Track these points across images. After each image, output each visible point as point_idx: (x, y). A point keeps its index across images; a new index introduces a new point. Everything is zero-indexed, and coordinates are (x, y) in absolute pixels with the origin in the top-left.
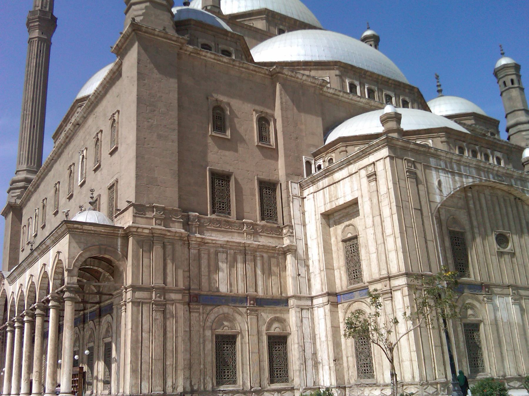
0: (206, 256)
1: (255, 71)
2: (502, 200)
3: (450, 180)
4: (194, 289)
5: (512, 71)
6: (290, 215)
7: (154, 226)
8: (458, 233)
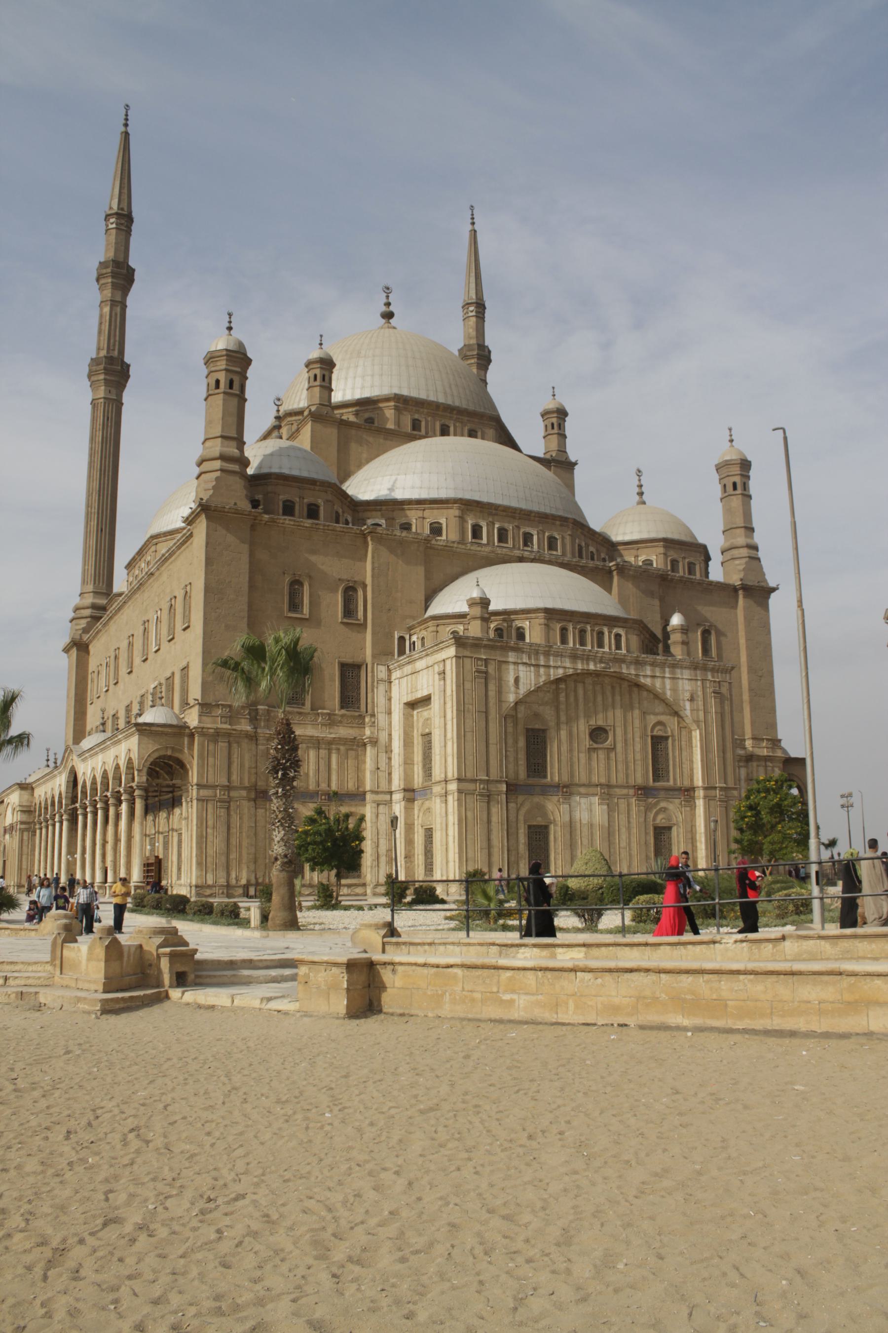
2: (609, 688)
3: (533, 674)
5: (736, 470)
6: (373, 702)
7: (220, 726)
8: (539, 730)
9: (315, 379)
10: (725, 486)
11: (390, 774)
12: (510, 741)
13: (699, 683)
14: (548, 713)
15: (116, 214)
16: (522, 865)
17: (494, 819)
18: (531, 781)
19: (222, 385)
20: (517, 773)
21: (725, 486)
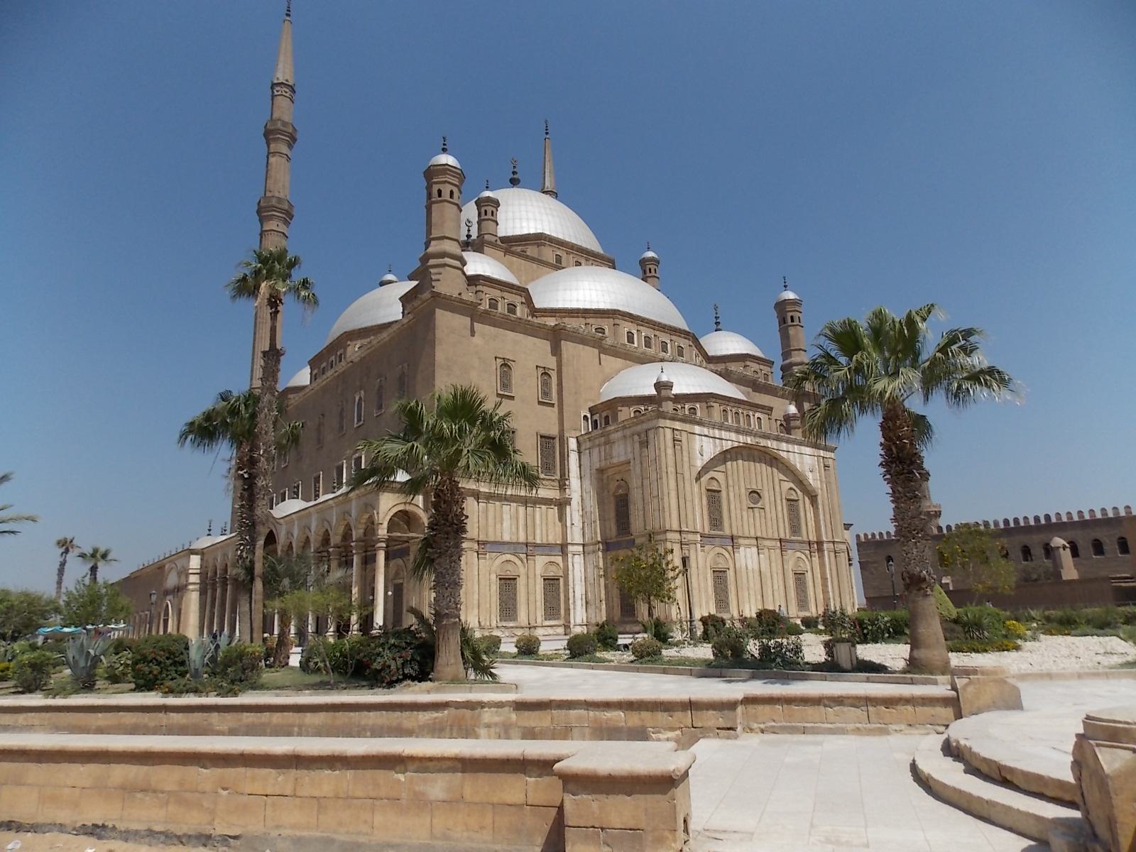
3: (712, 445)
8: (714, 491)
9: (486, 214)
14: (720, 477)
15: (282, 83)
16: (711, 605)
18: (713, 532)
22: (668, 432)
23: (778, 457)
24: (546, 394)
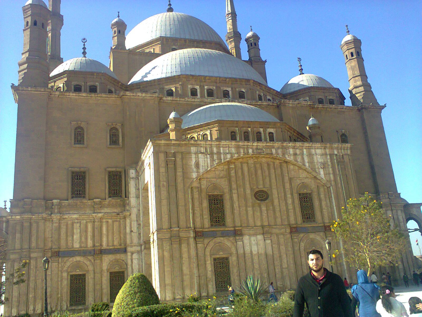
0: (65, 227)
1: (107, 97)
3: (209, 160)
4: (54, 249)
5: (352, 46)
9: (115, 33)
10: (347, 56)
11: (140, 234)
12: (197, 204)
13: (328, 157)
14: (223, 183)
16: (210, 286)
17: (185, 255)
19: (29, 24)
20: (203, 224)
21: (347, 56)
22: (162, 156)
23: (286, 160)
24: (114, 140)
